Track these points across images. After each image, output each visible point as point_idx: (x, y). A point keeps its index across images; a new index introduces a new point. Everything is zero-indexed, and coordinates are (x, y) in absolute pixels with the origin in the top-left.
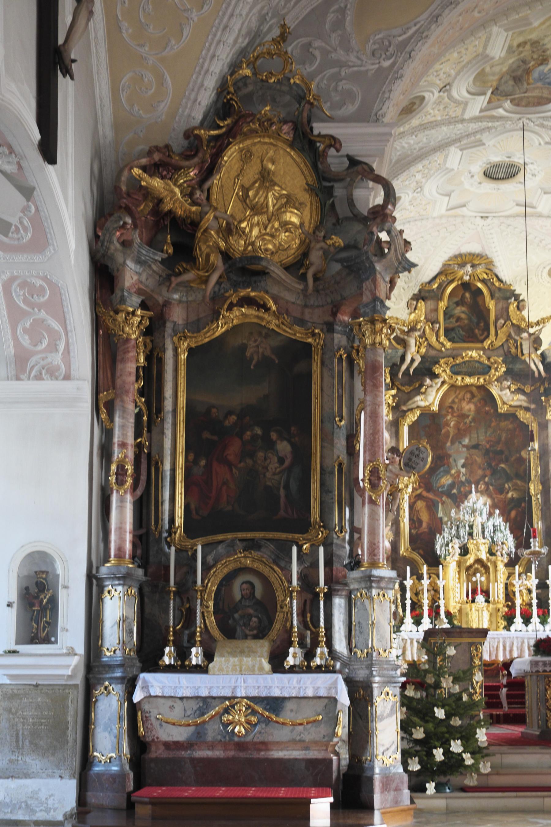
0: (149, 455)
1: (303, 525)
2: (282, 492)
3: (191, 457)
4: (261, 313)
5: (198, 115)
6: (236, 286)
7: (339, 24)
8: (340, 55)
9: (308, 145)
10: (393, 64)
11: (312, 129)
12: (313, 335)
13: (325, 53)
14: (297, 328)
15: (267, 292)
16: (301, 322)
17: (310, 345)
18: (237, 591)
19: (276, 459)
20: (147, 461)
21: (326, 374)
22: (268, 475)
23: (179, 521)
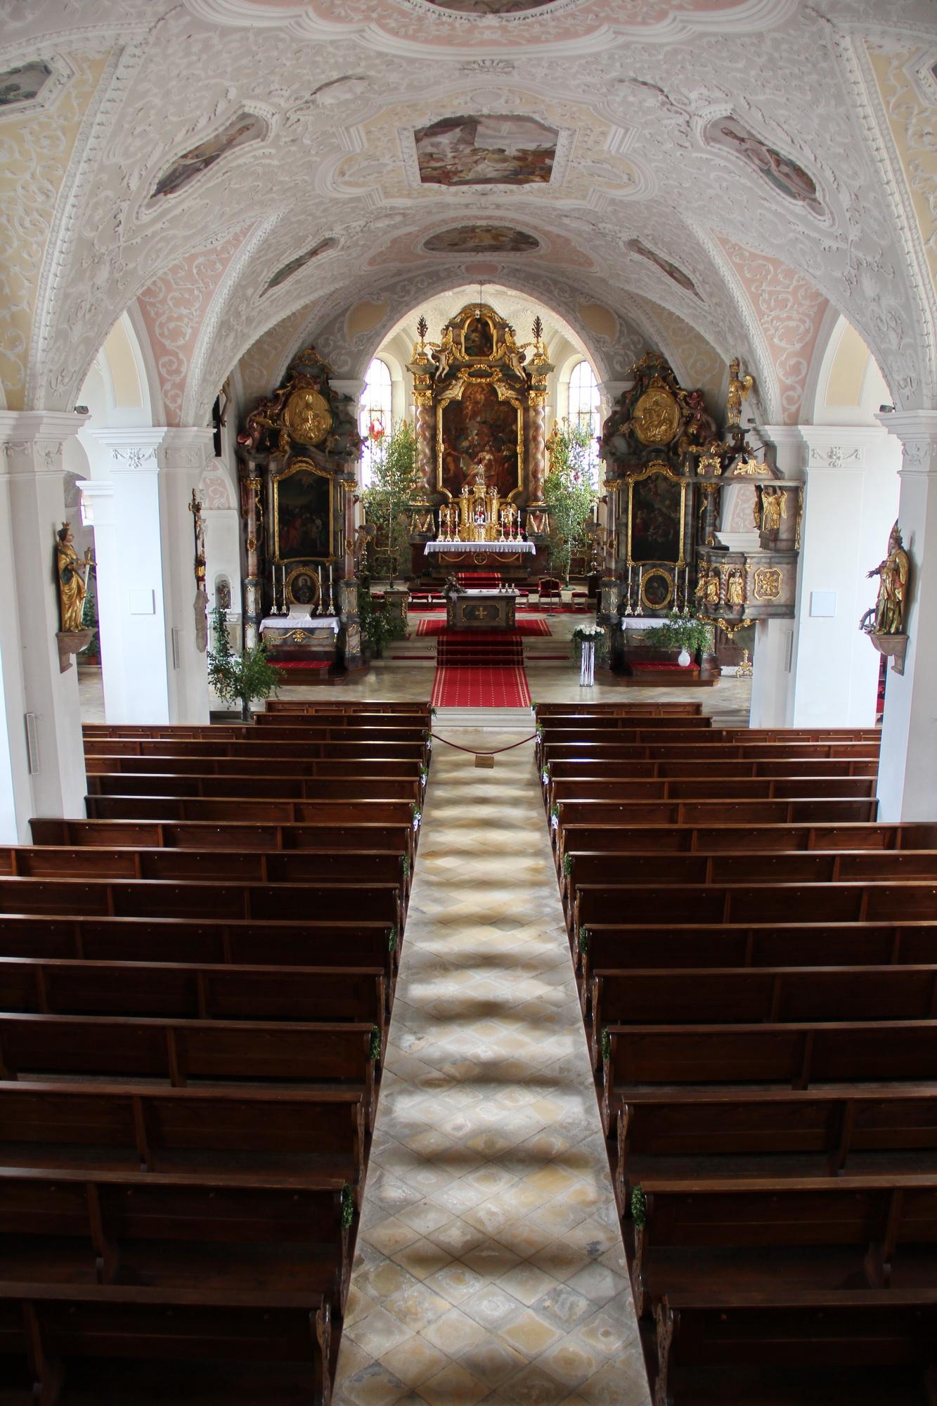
5: (278, 384)
6: (296, 456)
9: (327, 393)
16: (324, 469)
18: (300, 584)
23: (277, 553)
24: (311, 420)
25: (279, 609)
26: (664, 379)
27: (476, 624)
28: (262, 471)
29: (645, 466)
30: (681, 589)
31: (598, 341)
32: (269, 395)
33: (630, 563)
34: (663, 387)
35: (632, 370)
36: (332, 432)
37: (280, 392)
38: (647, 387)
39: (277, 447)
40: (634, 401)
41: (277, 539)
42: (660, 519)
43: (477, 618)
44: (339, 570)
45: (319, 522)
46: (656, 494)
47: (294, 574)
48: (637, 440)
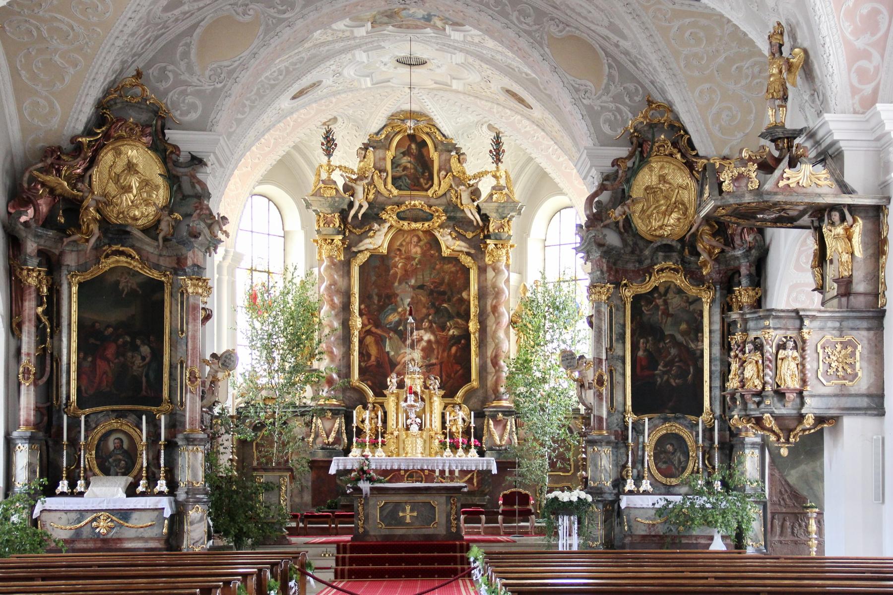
0: (52, 354)
1: (157, 400)
2: (144, 379)
3: (82, 355)
4: (129, 260)
7: (186, 55)
8: (185, 77)
10: (224, 86)
11: (164, 135)
12: (165, 275)
13: (176, 75)
14: (154, 271)
15: (132, 247)
16: (157, 267)
17: (163, 282)
18: (111, 446)
19: (140, 357)
20: (48, 359)
21: (174, 302)
22: (135, 368)
23: (74, 397)
24: (131, 181)
25: (72, 485)
26: (675, 144)
27: (400, 531)
28: (51, 263)
29: (649, 271)
30: (708, 453)
31: (577, 90)
32: (66, 145)
33: (630, 418)
34: (671, 155)
35: (626, 130)
36: (169, 208)
37: (85, 140)
38: (649, 156)
39: (79, 227)
40: (633, 172)
41: (74, 375)
42: (673, 351)
43: (401, 522)
44: (175, 425)
45: (145, 350)
46: (666, 313)
47: (101, 430)
48: (636, 235)
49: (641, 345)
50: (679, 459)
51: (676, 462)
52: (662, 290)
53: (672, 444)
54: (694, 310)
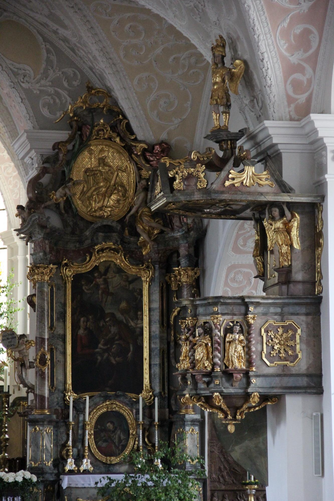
46: (106, 292)
49: (82, 323)
50: (119, 437)
51: (116, 441)
52: (102, 269)
53: (112, 422)
54: (134, 288)
